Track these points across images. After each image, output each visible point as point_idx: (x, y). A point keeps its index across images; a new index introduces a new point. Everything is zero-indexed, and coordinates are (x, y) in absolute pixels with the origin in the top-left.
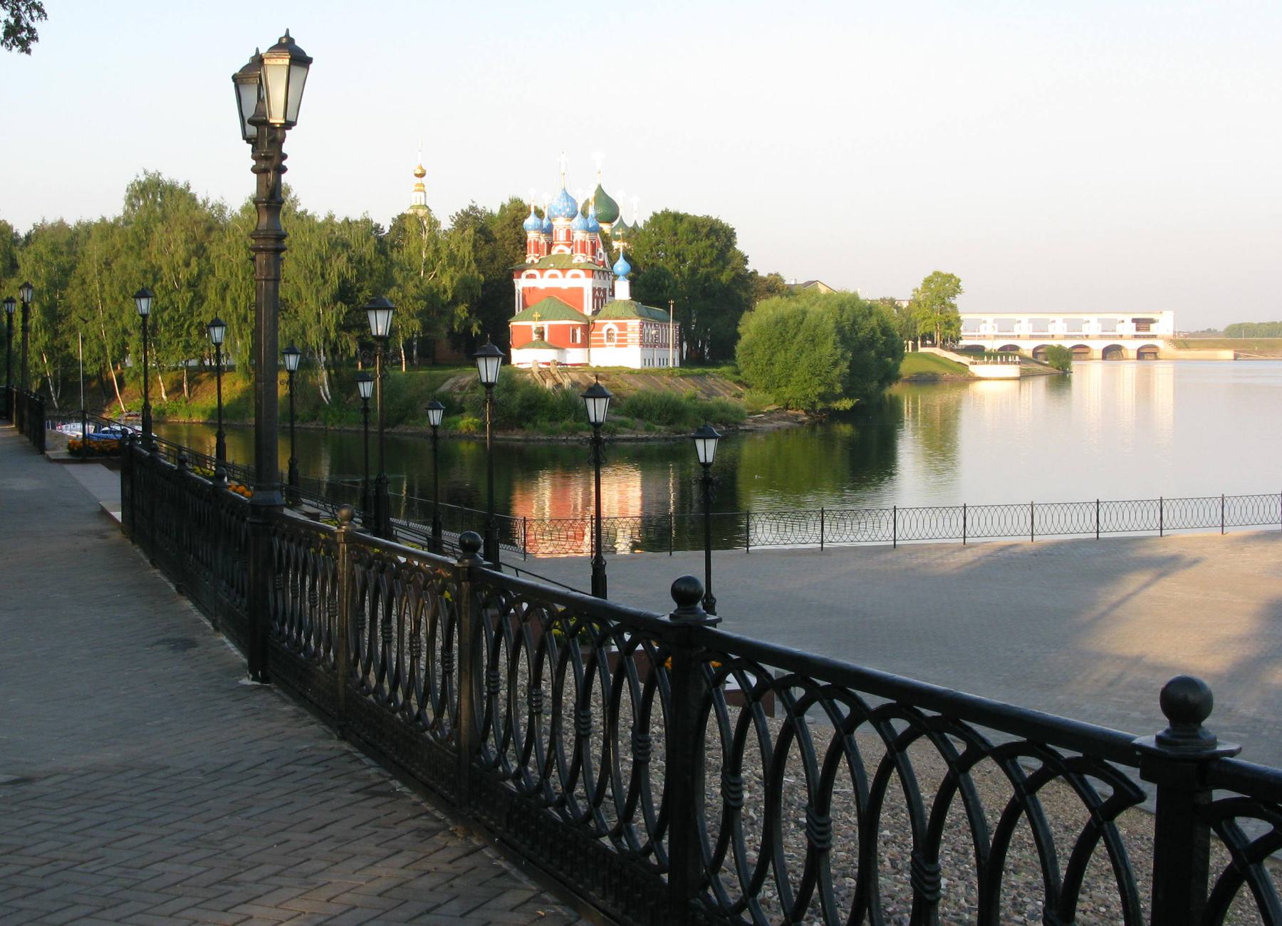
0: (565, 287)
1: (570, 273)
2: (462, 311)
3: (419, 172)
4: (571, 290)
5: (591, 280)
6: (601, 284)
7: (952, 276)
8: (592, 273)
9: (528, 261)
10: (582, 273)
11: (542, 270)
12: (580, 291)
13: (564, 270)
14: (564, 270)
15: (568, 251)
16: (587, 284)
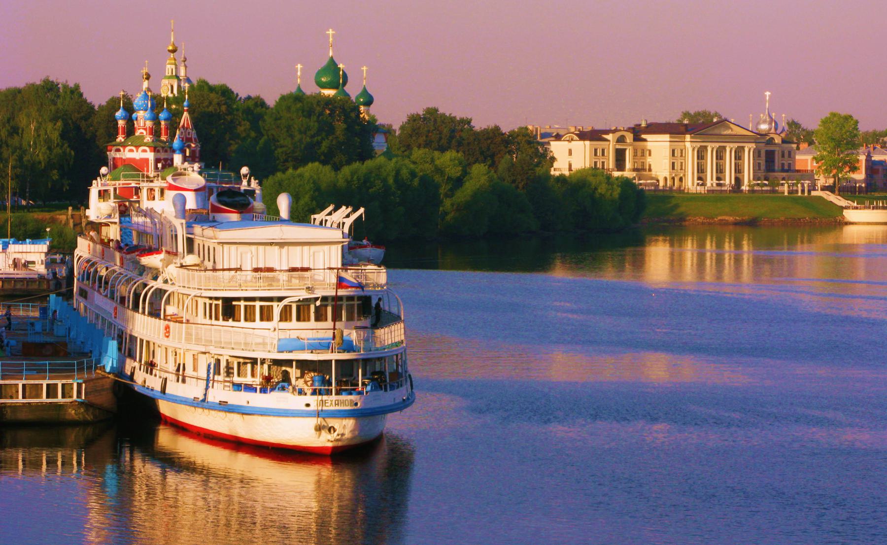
0: (138, 158)
1: (141, 148)
2: (55, 175)
3: (170, 48)
4: (141, 160)
5: (153, 154)
6: (163, 155)
7: (848, 118)
8: (155, 150)
9: (118, 140)
10: (147, 149)
11: (124, 147)
12: (147, 160)
13: (137, 147)
14: (137, 147)
15: (145, 132)
16: (150, 156)
